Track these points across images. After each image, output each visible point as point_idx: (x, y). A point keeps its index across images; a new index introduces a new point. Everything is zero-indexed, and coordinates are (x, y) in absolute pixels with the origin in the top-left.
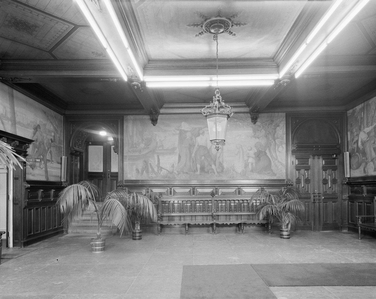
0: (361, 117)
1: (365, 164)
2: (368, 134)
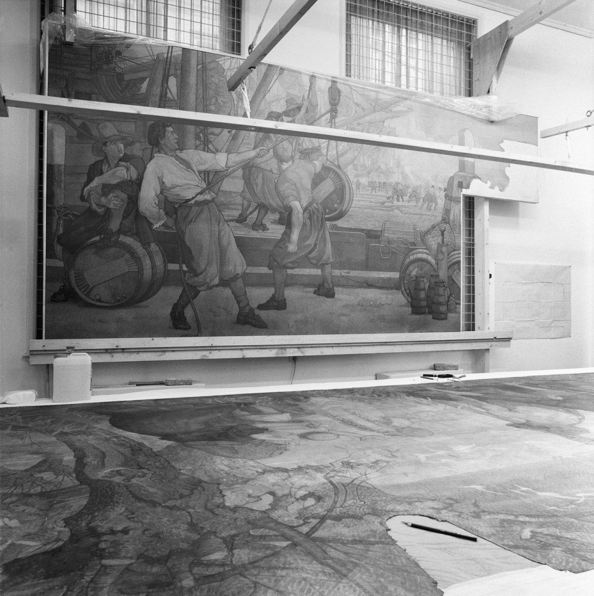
1: (184, 290)
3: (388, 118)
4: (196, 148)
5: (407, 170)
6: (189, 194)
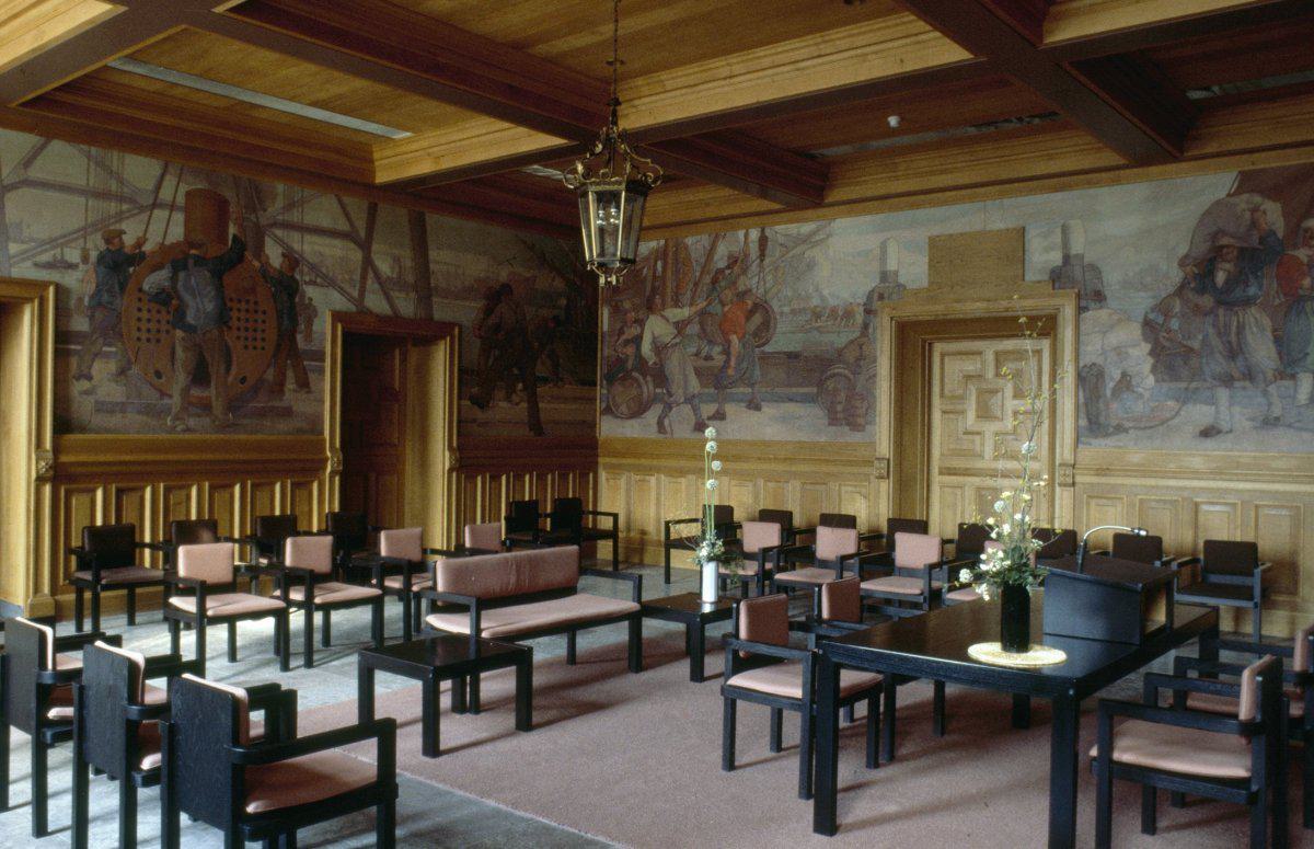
0: (654, 273)
2: (680, 326)
3: (807, 250)
4: (672, 307)
5: (826, 292)
6: (667, 340)
